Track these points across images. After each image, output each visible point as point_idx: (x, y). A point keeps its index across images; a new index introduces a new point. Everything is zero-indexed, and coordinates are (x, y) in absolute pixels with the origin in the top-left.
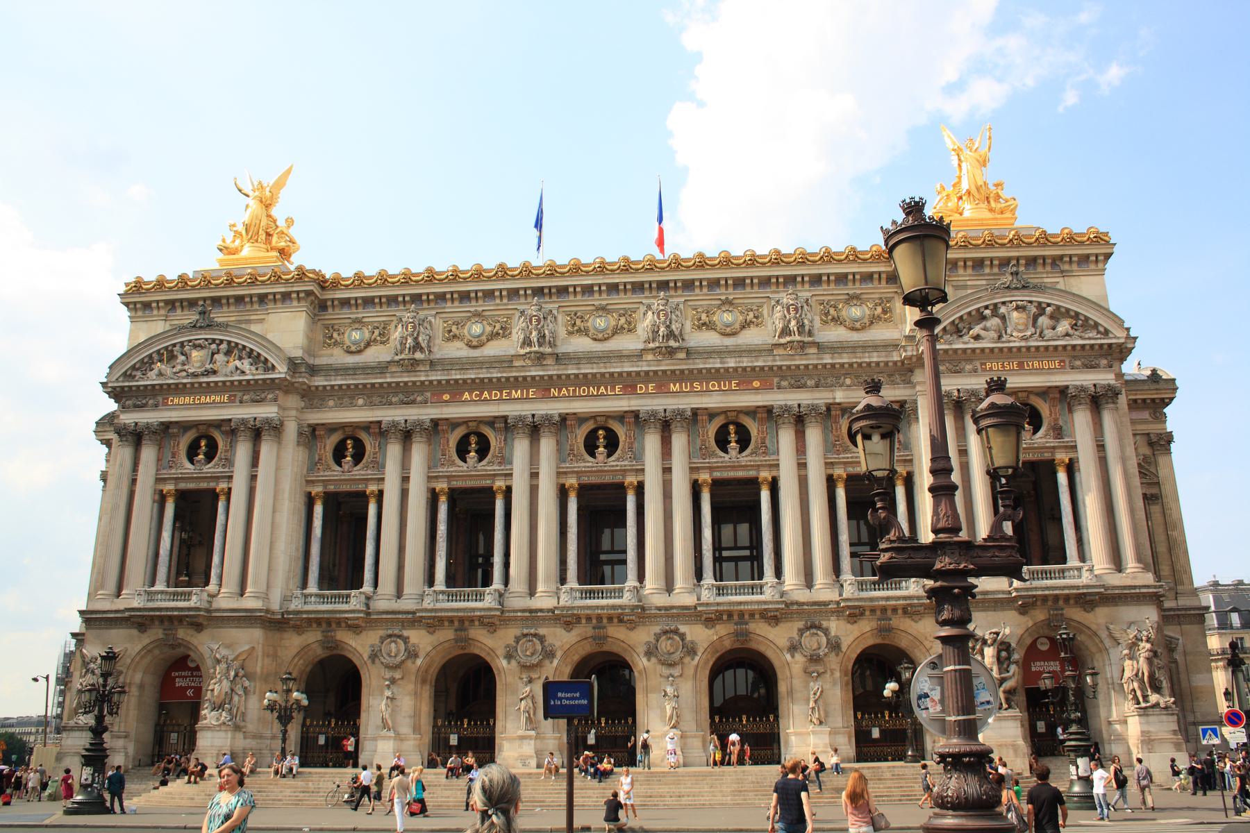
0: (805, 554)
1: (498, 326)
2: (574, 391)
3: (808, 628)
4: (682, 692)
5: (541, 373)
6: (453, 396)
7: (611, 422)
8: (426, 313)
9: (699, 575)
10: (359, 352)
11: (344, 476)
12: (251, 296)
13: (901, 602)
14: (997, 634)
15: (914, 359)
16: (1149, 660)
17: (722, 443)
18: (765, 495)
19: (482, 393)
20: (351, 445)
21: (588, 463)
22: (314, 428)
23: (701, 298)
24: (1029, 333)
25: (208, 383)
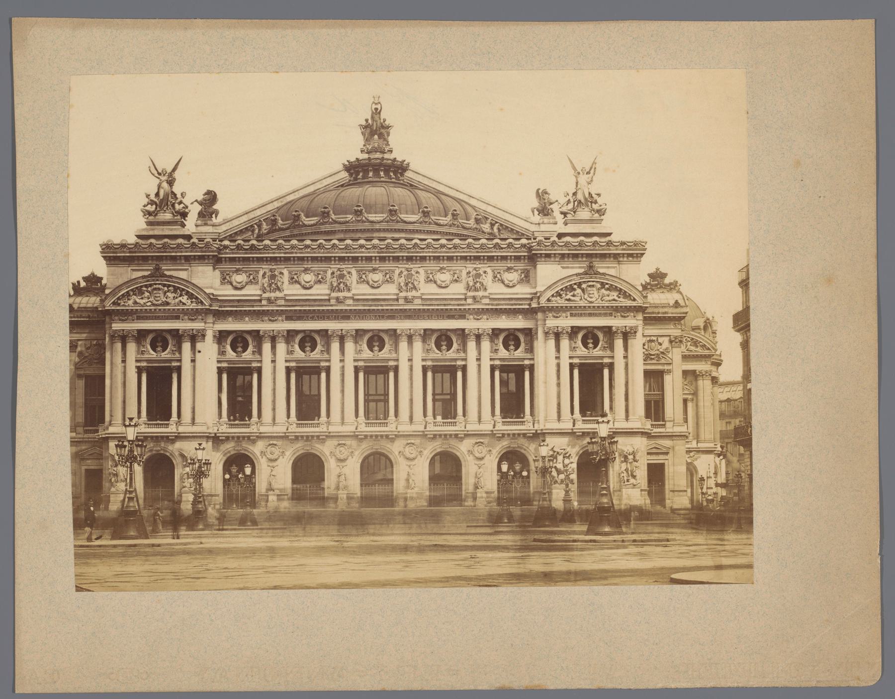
1: (320, 277)
9: (425, 415)
20: (239, 341)
22: (220, 332)
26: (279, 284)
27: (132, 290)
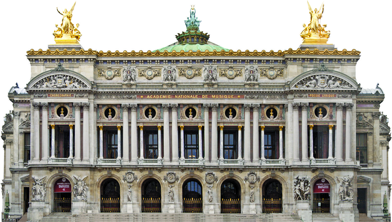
0: (251, 151)
1: (157, 72)
2: (182, 96)
3: (251, 174)
4: (213, 192)
5: (172, 91)
6: (144, 96)
7: (194, 106)
8: (133, 67)
9: (219, 156)
10: (111, 79)
11: (109, 121)
12: (74, 59)
13: (278, 167)
14: (305, 178)
15: (288, 92)
16: (347, 188)
17: (227, 114)
18: (240, 132)
19: (153, 96)
21: (187, 119)
22: (98, 105)
23: (223, 66)
24: (324, 86)
25: (64, 90)
26: (133, 76)
27: (45, 78)
